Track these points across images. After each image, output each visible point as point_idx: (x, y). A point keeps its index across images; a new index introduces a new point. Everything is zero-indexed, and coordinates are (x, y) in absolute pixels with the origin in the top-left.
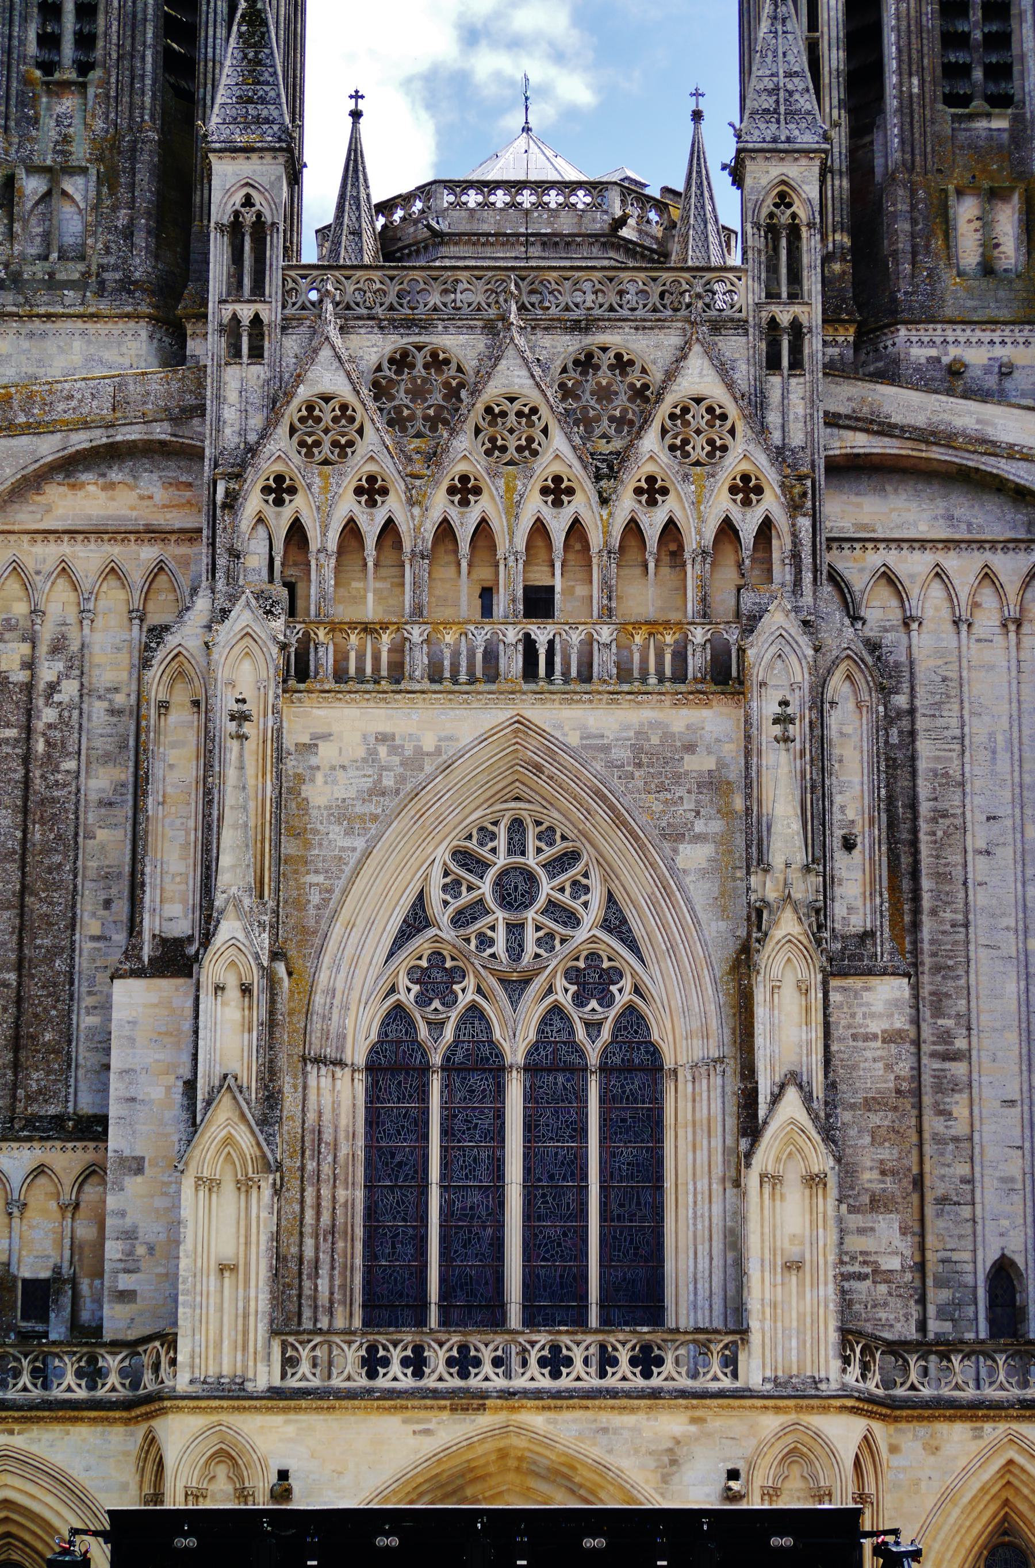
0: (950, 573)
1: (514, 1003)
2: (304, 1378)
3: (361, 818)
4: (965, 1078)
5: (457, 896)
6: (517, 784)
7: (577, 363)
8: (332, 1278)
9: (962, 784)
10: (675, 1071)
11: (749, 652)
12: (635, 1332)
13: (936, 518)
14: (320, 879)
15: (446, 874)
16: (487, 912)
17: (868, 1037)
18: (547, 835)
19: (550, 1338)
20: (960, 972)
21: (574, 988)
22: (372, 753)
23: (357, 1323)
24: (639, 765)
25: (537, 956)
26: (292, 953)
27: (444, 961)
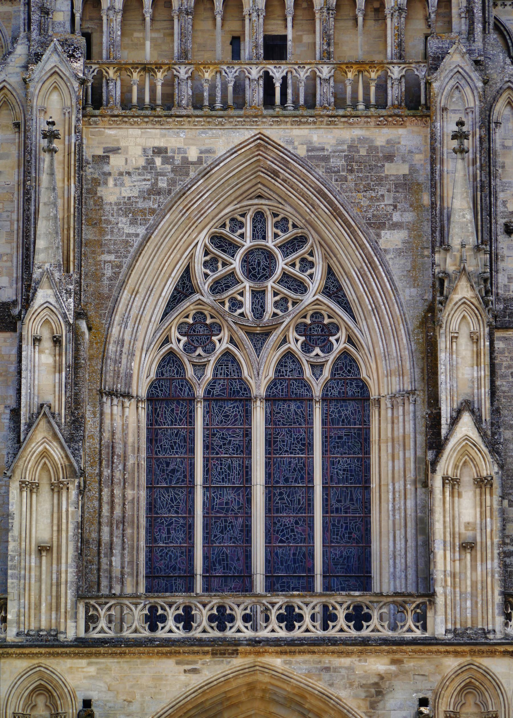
1: (258, 350)
2: (102, 631)
3: (143, 211)
5: (215, 270)
6: (260, 186)
8: (123, 556)
10: (379, 401)
11: (434, 85)
12: (349, 596)
14: (112, 257)
15: (206, 254)
16: (238, 282)
19: (286, 600)
21: (302, 339)
22: (150, 162)
23: (142, 589)
24: (351, 171)
25: (275, 314)
26: (91, 313)
27: (205, 318)
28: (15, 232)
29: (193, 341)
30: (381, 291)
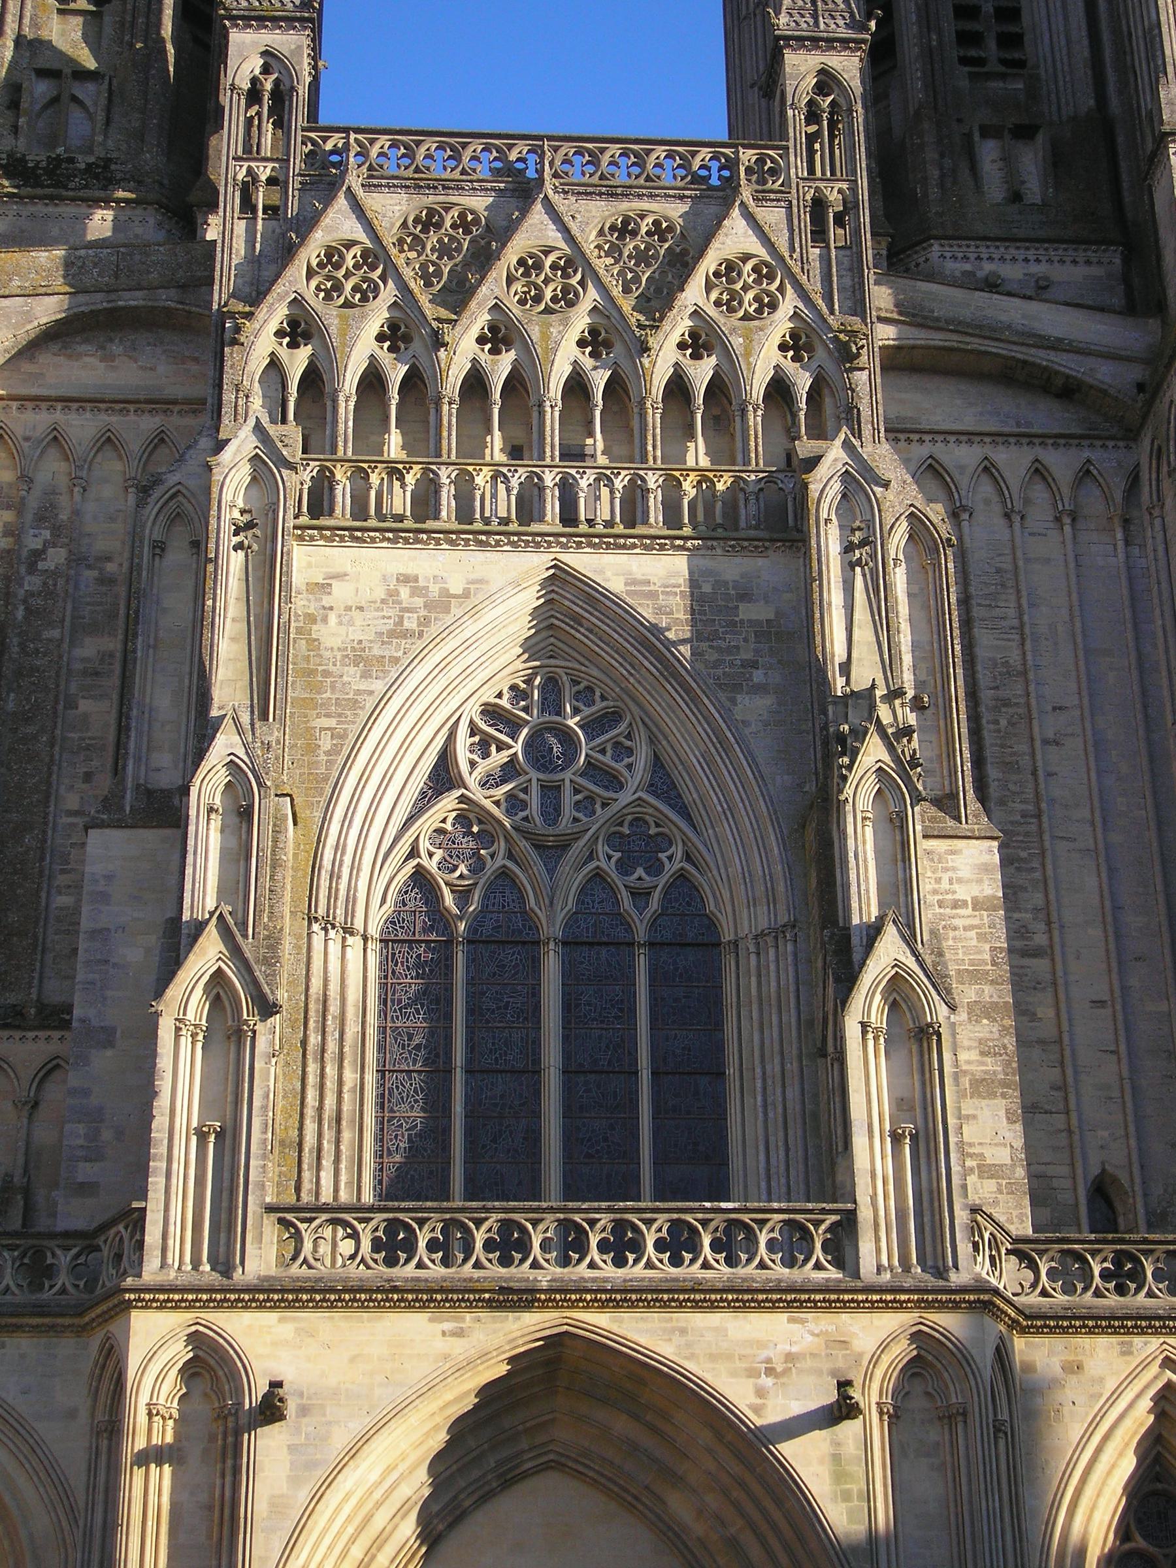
0: (1000, 466)
1: (551, 871)
4: (1048, 977)
5: (486, 755)
6: (552, 640)
7: (613, 228)
9: (1025, 673)
10: (736, 944)
13: (981, 414)
14: (332, 722)
17: (956, 905)
18: (585, 695)
20: (1036, 864)
21: (618, 855)
25: (576, 820)
28: (186, 690)
29: (451, 857)
30: (737, 781)
